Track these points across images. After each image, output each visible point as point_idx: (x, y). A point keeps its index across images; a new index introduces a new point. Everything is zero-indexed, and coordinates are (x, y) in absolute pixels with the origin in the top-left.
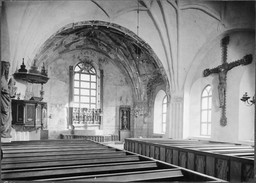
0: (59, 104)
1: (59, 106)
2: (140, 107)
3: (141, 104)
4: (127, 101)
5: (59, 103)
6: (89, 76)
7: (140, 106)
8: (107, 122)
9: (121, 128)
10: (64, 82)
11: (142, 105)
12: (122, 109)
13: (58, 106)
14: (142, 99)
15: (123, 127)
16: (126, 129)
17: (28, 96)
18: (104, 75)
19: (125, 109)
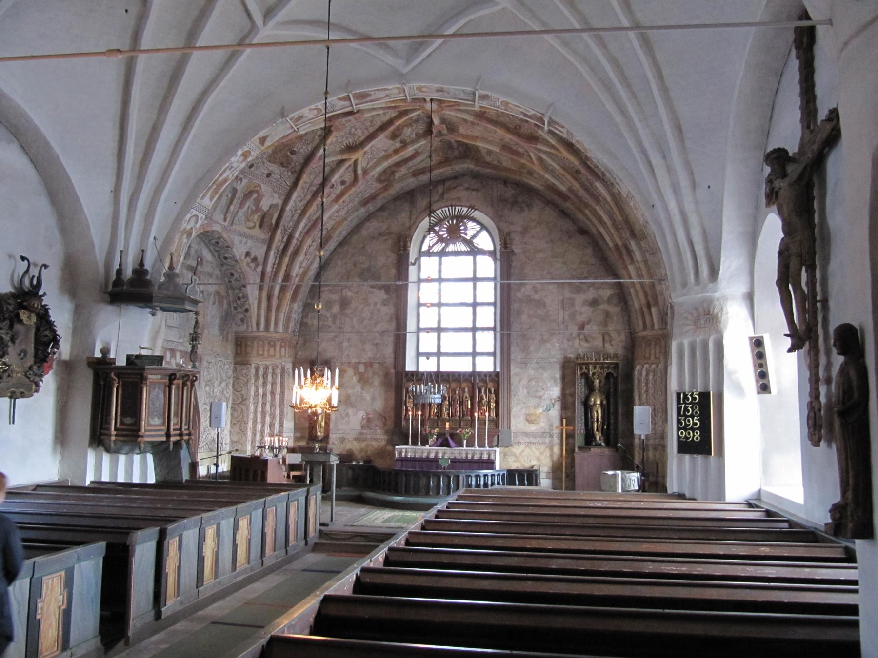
0: (365, 364)
1: (365, 368)
2: (652, 357)
3: (653, 343)
4: (607, 337)
5: (363, 361)
6: (470, 259)
7: (653, 352)
8: (527, 420)
9: (579, 440)
10: (383, 291)
11: (658, 350)
12: (584, 370)
13: (362, 368)
14: (656, 327)
15: (589, 439)
16: (600, 445)
17: (269, 343)
18: (516, 251)
19: (595, 368)
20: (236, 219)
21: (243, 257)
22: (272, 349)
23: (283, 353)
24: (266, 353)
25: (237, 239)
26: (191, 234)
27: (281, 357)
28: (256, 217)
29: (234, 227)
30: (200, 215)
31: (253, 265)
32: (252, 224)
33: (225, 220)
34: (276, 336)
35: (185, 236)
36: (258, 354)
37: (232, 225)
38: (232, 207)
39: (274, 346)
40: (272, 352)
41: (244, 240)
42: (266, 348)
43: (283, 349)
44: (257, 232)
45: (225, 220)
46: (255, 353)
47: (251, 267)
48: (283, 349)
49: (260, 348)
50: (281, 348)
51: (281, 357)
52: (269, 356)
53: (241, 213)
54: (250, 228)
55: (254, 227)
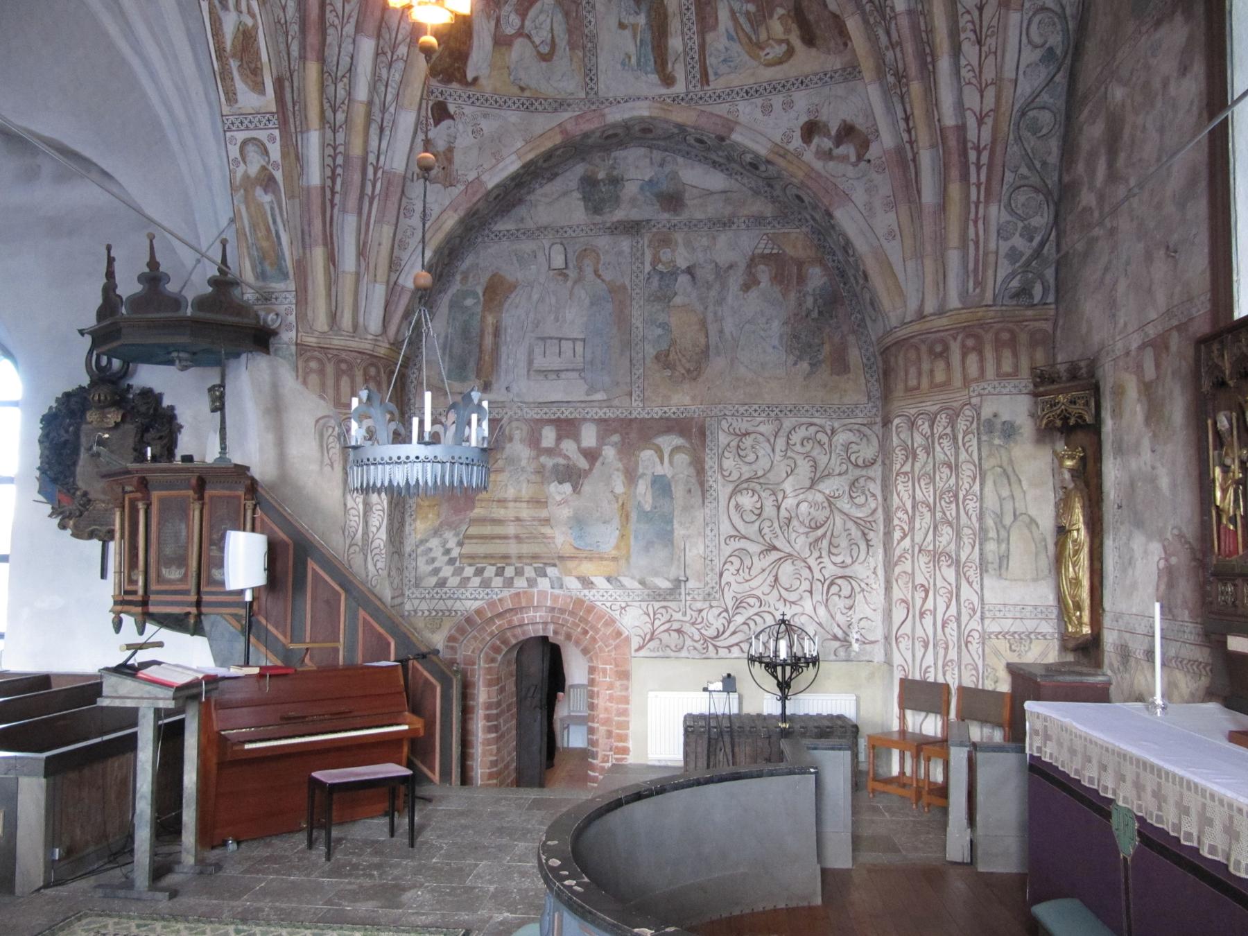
17: (931, 351)
20: (711, 61)
21: (797, 142)
22: (940, 365)
23: (973, 370)
24: (925, 382)
25: (746, 111)
26: (272, 179)
27: (966, 382)
28: (777, 27)
29: (717, 84)
30: (262, 135)
31: (848, 149)
32: (780, 50)
33: (668, 80)
34: (944, 322)
35: (259, 191)
36: (907, 389)
37: (705, 79)
38: (675, 43)
39: (944, 354)
40: (940, 377)
41: (777, 100)
42: (926, 366)
43: (973, 359)
44: (807, 61)
45: (668, 80)
46: (901, 386)
47: (844, 159)
48: (973, 359)
49: (913, 371)
50: (964, 356)
51: (966, 382)
52: (933, 386)
53: (719, 41)
54: (780, 62)
55: (790, 52)
